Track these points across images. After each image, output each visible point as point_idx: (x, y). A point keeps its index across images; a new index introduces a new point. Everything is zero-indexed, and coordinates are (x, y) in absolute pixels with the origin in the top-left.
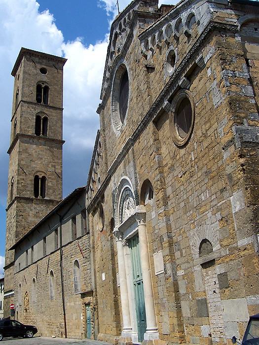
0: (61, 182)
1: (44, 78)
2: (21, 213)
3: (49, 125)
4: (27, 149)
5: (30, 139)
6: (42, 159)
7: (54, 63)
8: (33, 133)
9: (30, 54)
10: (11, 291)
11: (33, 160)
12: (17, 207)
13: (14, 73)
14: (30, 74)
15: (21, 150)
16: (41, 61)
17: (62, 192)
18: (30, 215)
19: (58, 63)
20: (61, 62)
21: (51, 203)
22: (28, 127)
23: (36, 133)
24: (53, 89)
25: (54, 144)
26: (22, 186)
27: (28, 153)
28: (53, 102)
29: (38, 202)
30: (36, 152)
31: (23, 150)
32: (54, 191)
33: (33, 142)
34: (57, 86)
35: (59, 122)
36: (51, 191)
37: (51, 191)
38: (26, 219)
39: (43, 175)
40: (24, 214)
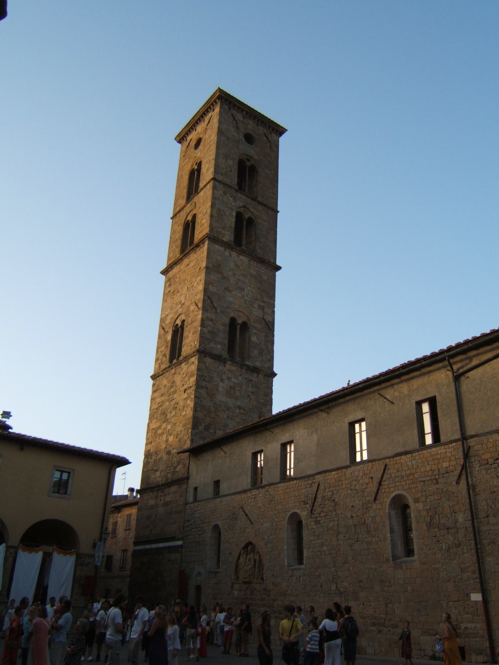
1: (251, 151)
2: (204, 384)
6: (243, 289)
7: (265, 130)
9: (230, 103)
10: (173, 539)
11: (230, 289)
12: (198, 369)
13: (181, 138)
14: (228, 138)
15: (211, 266)
18: (220, 389)
19: (271, 133)
20: (277, 131)
22: (224, 228)
23: (235, 243)
26: (209, 332)
30: (234, 275)
33: (230, 255)
37: (256, 352)
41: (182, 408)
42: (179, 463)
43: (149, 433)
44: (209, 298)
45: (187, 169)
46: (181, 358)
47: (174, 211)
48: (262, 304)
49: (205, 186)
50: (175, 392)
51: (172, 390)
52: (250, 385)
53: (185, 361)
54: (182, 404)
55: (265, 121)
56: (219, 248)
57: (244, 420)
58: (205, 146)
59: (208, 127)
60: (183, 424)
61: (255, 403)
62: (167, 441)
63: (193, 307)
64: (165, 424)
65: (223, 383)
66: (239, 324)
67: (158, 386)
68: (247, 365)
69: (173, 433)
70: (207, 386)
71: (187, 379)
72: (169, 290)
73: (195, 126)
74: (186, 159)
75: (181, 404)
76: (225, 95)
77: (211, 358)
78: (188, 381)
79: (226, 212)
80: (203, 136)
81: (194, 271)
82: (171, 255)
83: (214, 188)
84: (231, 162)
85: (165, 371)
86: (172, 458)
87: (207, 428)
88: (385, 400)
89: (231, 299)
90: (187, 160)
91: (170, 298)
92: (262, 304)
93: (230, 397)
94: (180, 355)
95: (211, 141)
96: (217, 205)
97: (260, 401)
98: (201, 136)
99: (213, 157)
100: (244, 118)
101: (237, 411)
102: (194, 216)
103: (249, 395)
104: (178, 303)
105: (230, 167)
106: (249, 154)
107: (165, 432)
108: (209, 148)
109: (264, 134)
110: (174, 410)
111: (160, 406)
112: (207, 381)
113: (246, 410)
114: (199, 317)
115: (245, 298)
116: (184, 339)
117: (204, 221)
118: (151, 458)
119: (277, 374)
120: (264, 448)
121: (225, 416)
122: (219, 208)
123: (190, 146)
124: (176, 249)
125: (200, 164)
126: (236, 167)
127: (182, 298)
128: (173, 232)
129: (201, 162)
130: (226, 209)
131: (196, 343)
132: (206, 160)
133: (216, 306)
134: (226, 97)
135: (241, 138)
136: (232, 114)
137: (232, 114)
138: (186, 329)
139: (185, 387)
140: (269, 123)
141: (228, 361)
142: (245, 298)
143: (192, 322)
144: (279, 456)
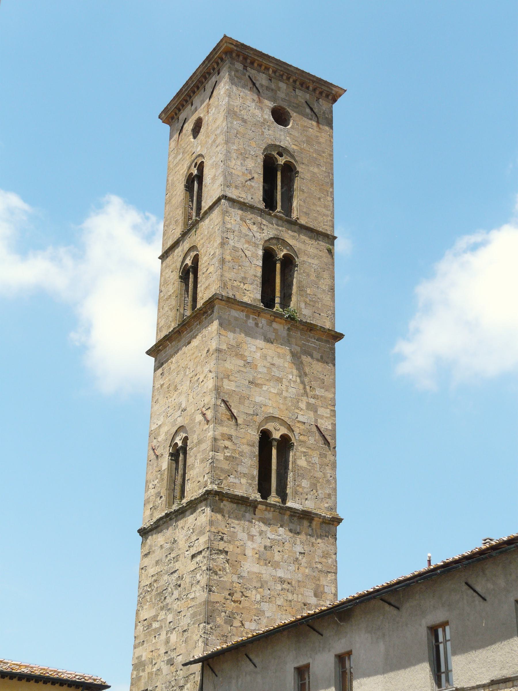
0: (332, 458)
2: (222, 545)
3: (300, 282)
4: (238, 346)
5: (248, 317)
7: (308, 96)
8: (255, 300)
9: (245, 58)
11: (259, 382)
14: (245, 121)
15: (224, 347)
16: (273, 86)
17: (335, 489)
18: (249, 552)
19: (318, 99)
20: (327, 96)
21: (306, 523)
22: (244, 280)
24: (308, 176)
25: (313, 343)
26: (226, 458)
27: (242, 357)
28: (307, 214)
29: (269, 515)
30: (265, 357)
31: (231, 347)
32: (314, 487)
33: (257, 325)
34: (318, 165)
35: (326, 275)
36: (305, 483)
37: (305, 483)
38: (235, 564)
39: (284, 431)
40: (230, 548)
41: (188, 585)
42: (187, 678)
43: (138, 627)
44: (223, 401)
45: (182, 172)
46: (185, 501)
47: (163, 245)
48: (312, 401)
49: (211, 208)
50: (176, 559)
51: (172, 555)
52: (298, 540)
53: (190, 508)
54: (188, 580)
55: (307, 80)
56: (237, 316)
57: (290, 601)
58: (208, 136)
59: (210, 103)
60: (191, 614)
61: (307, 571)
62: (167, 641)
63: (199, 418)
64: (164, 612)
65: (252, 541)
66: (275, 440)
67: (151, 546)
68: (290, 509)
69: (177, 629)
70: (226, 549)
71: (195, 538)
72: (162, 383)
73: (190, 97)
74: (177, 154)
75: (188, 579)
76: (235, 46)
77: (231, 502)
78: (196, 542)
79: (247, 252)
80: (204, 115)
81: (200, 354)
82: (162, 323)
83: (225, 213)
84: (250, 164)
85: (161, 522)
86: (177, 671)
87: (230, 620)
88: (475, 594)
89: (258, 399)
90: (181, 156)
91: (164, 397)
92: (312, 401)
93: (266, 564)
94: (182, 496)
95: (218, 127)
96: (231, 242)
97: (315, 566)
98: (202, 116)
99: (221, 157)
100: (270, 80)
101: (279, 587)
102: (196, 260)
103: (297, 559)
104: (177, 408)
105: (250, 173)
106: (282, 144)
107: (163, 626)
108: (214, 141)
109: (306, 102)
110: (176, 589)
111: (155, 581)
112: (226, 540)
113: (293, 583)
114: (209, 434)
115: (285, 394)
116: (189, 471)
117: (211, 269)
118: (144, 670)
119: (342, 520)
120: (310, 661)
121: (258, 597)
122: (234, 247)
123: (184, 131)
124: (169, 312)
125: (201, 167)
126: (261, 170)
127: (183, 400)
128: (164, 283)
129: (202, 163)
130: (246, 246)
131: (206, 478)
132: (211, 162)
133: (235, 415)
134: (238, 50)
135: (266, 117)
136: (249, 76)
137: (249, 76)
138: (190, 453)
139: (193, 551)
140: (313, 82)
141: (259, 504)
142: (285, 394)
143: (200, 442)
144: (333, 675)
